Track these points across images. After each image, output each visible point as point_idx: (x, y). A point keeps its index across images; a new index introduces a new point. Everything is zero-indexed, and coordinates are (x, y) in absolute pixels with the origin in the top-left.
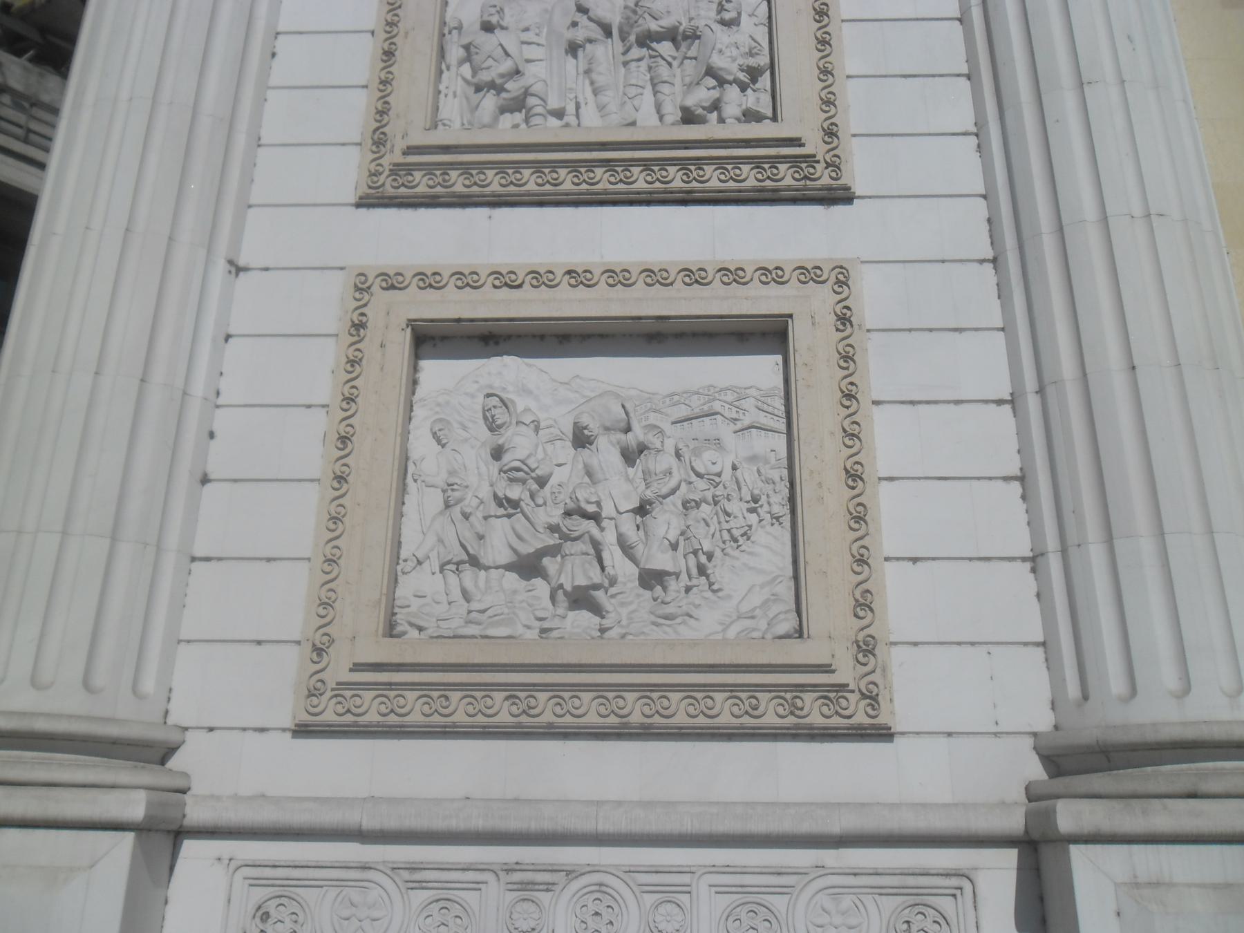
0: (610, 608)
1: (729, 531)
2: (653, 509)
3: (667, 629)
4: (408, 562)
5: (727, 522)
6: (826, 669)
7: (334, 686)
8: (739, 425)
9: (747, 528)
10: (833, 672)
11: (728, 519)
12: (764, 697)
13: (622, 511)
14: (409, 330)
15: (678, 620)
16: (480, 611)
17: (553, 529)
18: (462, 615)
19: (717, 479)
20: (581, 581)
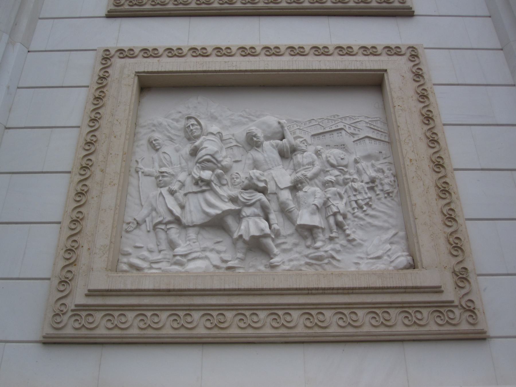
0: (276, 250)
1: (356, 202)
2: (303, 187)
3: (318, 267)
4: (130, 224)
5: (355, 195)
6: (437, 290)
7: (73, 307)
8: (356, 139)
9: (368, 200)
10: (442, 292)
11: (355, 193)
12: (393, 312)
13: (282, 187)
14: (136, 78)
15: (326, 261)
16: (181, 256)
17: (234, 200)
18: (169, 259)
19: (346, 170)
20: (254, 232)
